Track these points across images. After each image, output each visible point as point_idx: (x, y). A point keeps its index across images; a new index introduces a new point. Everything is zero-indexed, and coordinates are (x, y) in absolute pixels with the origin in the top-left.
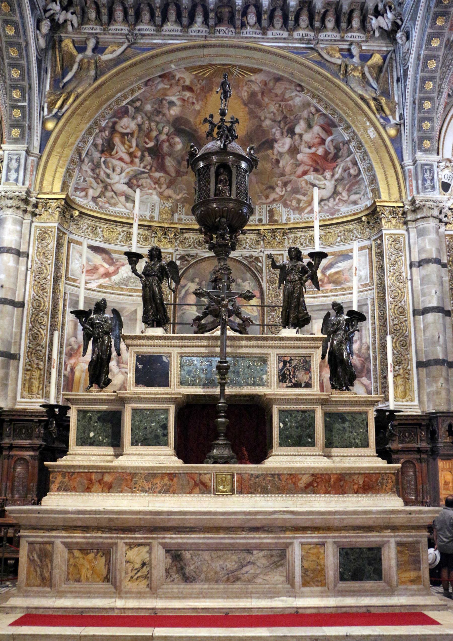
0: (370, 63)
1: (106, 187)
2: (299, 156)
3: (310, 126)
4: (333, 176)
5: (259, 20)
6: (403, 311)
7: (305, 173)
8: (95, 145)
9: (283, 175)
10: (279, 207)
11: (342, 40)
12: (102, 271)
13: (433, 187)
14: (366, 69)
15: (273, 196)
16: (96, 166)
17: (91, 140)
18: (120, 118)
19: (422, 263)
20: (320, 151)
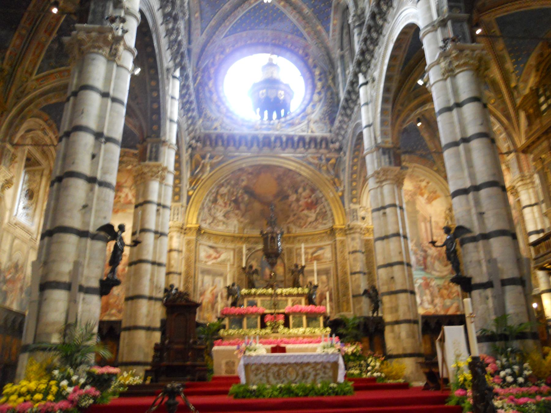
0: (331, 162)
1: (214, 218)
2: (301, 203)
3: (304, 190)
4: (315, 211)
5: (281, 145)
6: (345, 273)
7: (303, 210)
8: (209, 200)
9: (293, 211)
10: (292, 226)
11: (317, 153)
12: (213, 257)
13: (357, 219)
14: (329, 166)
15: (289, 221)
16: (210, 209)
17: (208, 199)
18: (221, 187)
19: (354, 252)
20: (309, 201)
